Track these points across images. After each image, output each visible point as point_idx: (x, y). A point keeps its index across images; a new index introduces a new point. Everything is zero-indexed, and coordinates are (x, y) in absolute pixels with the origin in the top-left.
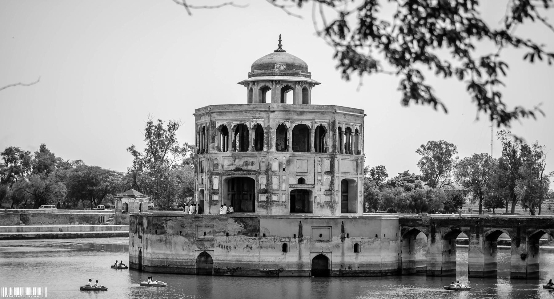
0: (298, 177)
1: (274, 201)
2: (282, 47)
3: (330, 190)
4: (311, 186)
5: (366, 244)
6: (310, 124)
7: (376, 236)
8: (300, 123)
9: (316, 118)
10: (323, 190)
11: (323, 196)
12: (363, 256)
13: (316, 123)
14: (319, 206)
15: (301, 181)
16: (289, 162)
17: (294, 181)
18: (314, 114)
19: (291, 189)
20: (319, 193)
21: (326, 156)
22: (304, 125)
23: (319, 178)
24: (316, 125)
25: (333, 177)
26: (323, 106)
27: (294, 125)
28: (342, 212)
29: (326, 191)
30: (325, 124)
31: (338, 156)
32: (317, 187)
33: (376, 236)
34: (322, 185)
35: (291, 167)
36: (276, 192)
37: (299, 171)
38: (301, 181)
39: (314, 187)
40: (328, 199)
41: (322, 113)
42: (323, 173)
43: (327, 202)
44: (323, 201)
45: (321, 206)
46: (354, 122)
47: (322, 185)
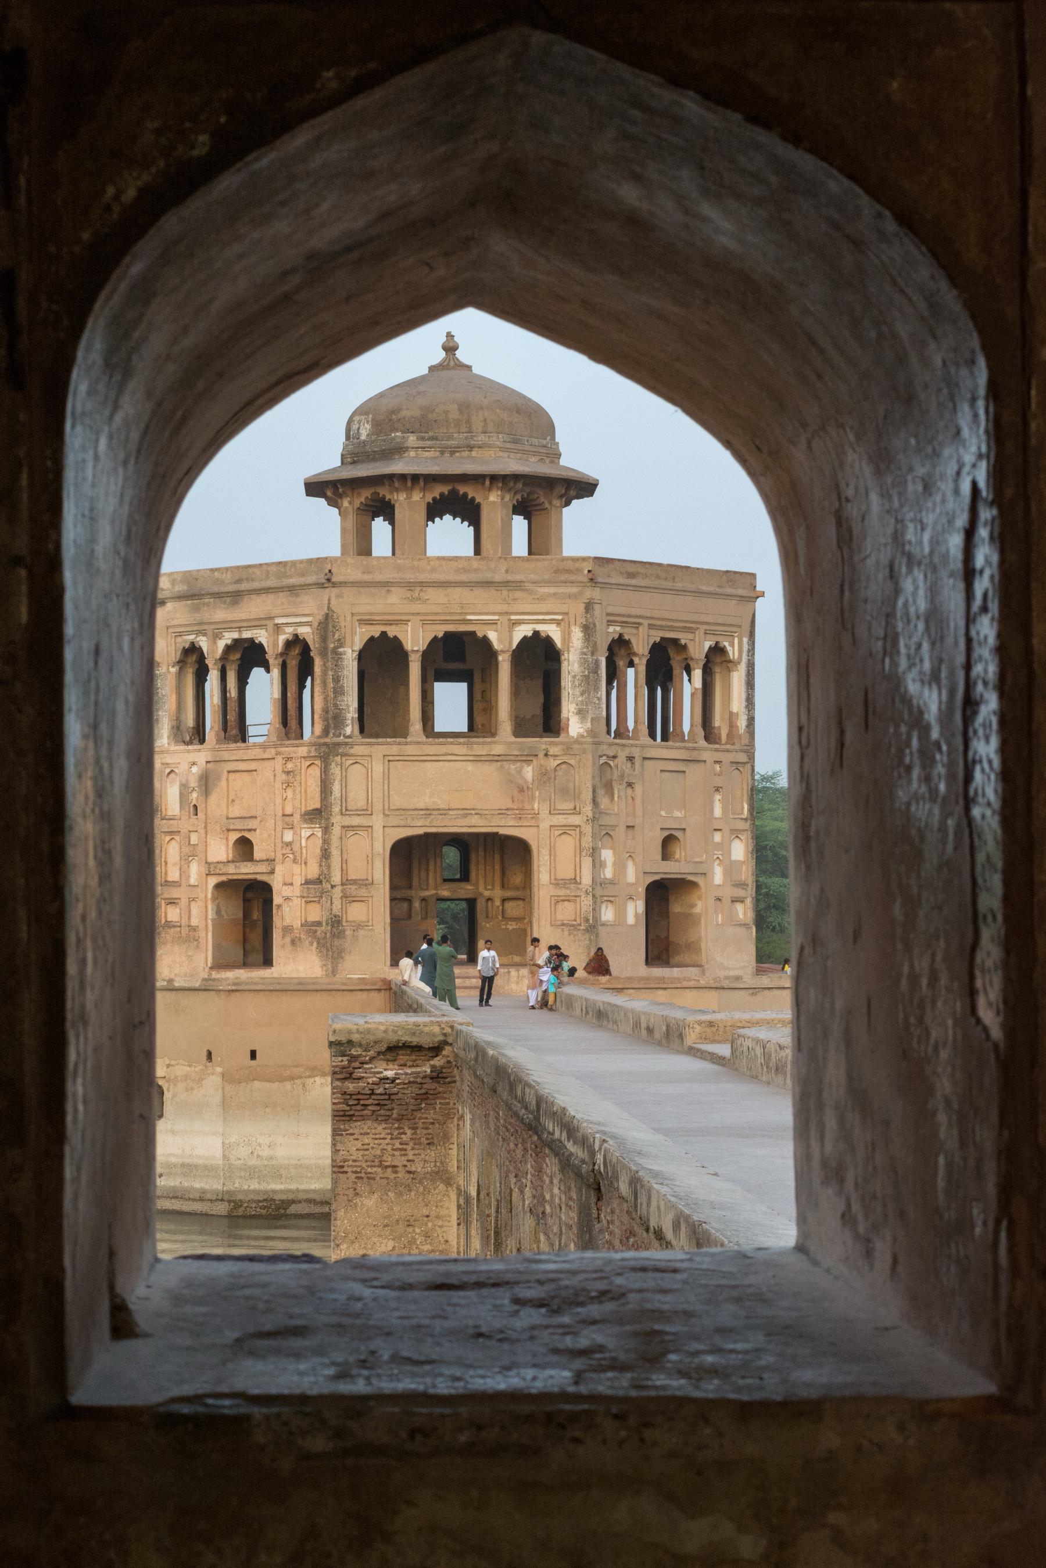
0: (234, 837)
1: (169, 925)
2: (458, 354)
3: (318, 881)
4: (262, 868)
5: (181, 1086)
6: (262, 637)
7: (209, 1055)
8: (236, 635)
9: (277, 611)
10: (298, 881)
11: (297, 902)
12: (173, 1132)
13: (278, 628)
14: (288, 940)
15: (244, 847)
16: (207, 782)
17: (220, 850)
18: (271, 596)
19: (213, 881)
20: (287, 891)
21: (303, 751)
22: (251, 641)
23: (288, 836)
24: (282, 639)
25: (327, 830)
26: (294, 563)
27: (221, 645)
28: (649, 961)
29: (307, 882)
30: (304, 631)
31: (358, 750)
32: (279, 869)
33: (209, 1055)
34: (295, 861)
35: (213, 798)
36: (175, 893)
37: (236, 811)
38: (244, 847)
39: (272, 872)
40: (315, 913)
41: (292, 590)
42: (297, 817)
43: (311, 927)
44: (297, 924)
45: (293, 942)
46: (504, 608)
47: (295, 861)
